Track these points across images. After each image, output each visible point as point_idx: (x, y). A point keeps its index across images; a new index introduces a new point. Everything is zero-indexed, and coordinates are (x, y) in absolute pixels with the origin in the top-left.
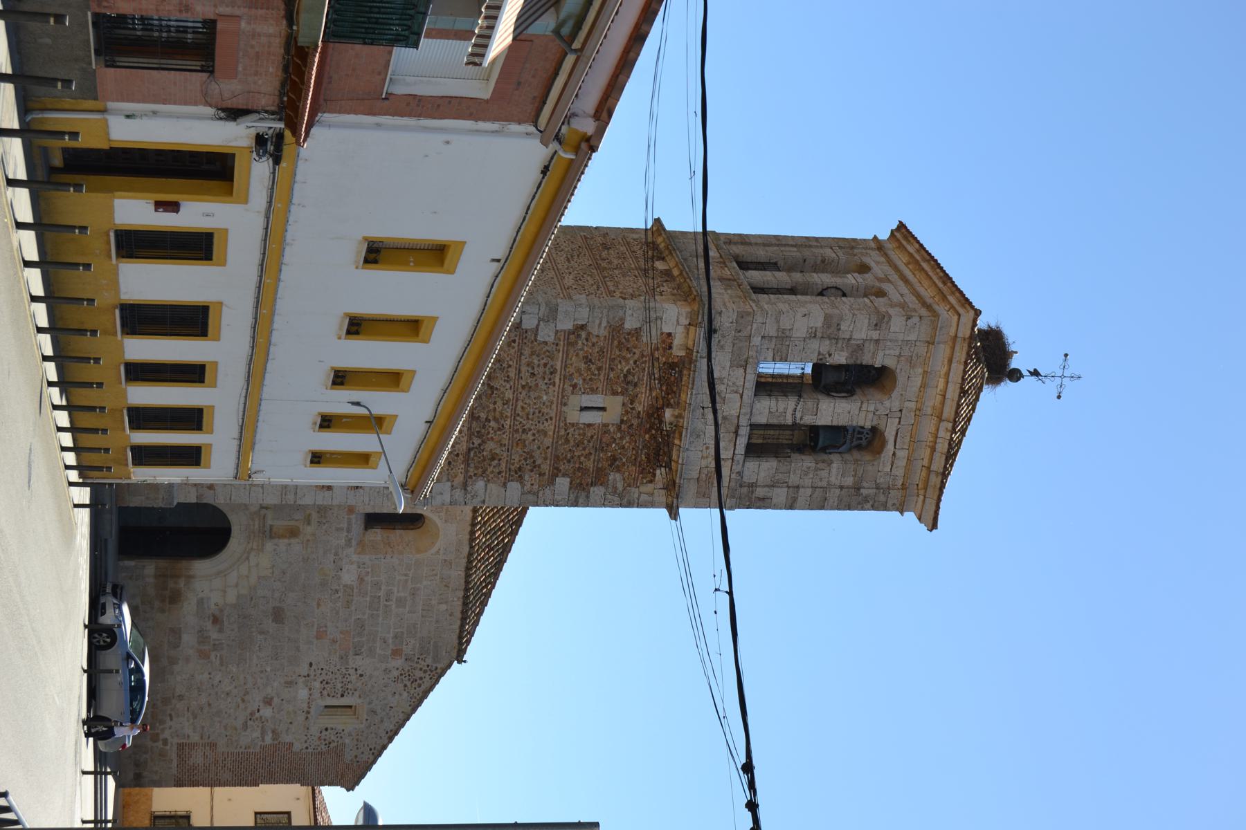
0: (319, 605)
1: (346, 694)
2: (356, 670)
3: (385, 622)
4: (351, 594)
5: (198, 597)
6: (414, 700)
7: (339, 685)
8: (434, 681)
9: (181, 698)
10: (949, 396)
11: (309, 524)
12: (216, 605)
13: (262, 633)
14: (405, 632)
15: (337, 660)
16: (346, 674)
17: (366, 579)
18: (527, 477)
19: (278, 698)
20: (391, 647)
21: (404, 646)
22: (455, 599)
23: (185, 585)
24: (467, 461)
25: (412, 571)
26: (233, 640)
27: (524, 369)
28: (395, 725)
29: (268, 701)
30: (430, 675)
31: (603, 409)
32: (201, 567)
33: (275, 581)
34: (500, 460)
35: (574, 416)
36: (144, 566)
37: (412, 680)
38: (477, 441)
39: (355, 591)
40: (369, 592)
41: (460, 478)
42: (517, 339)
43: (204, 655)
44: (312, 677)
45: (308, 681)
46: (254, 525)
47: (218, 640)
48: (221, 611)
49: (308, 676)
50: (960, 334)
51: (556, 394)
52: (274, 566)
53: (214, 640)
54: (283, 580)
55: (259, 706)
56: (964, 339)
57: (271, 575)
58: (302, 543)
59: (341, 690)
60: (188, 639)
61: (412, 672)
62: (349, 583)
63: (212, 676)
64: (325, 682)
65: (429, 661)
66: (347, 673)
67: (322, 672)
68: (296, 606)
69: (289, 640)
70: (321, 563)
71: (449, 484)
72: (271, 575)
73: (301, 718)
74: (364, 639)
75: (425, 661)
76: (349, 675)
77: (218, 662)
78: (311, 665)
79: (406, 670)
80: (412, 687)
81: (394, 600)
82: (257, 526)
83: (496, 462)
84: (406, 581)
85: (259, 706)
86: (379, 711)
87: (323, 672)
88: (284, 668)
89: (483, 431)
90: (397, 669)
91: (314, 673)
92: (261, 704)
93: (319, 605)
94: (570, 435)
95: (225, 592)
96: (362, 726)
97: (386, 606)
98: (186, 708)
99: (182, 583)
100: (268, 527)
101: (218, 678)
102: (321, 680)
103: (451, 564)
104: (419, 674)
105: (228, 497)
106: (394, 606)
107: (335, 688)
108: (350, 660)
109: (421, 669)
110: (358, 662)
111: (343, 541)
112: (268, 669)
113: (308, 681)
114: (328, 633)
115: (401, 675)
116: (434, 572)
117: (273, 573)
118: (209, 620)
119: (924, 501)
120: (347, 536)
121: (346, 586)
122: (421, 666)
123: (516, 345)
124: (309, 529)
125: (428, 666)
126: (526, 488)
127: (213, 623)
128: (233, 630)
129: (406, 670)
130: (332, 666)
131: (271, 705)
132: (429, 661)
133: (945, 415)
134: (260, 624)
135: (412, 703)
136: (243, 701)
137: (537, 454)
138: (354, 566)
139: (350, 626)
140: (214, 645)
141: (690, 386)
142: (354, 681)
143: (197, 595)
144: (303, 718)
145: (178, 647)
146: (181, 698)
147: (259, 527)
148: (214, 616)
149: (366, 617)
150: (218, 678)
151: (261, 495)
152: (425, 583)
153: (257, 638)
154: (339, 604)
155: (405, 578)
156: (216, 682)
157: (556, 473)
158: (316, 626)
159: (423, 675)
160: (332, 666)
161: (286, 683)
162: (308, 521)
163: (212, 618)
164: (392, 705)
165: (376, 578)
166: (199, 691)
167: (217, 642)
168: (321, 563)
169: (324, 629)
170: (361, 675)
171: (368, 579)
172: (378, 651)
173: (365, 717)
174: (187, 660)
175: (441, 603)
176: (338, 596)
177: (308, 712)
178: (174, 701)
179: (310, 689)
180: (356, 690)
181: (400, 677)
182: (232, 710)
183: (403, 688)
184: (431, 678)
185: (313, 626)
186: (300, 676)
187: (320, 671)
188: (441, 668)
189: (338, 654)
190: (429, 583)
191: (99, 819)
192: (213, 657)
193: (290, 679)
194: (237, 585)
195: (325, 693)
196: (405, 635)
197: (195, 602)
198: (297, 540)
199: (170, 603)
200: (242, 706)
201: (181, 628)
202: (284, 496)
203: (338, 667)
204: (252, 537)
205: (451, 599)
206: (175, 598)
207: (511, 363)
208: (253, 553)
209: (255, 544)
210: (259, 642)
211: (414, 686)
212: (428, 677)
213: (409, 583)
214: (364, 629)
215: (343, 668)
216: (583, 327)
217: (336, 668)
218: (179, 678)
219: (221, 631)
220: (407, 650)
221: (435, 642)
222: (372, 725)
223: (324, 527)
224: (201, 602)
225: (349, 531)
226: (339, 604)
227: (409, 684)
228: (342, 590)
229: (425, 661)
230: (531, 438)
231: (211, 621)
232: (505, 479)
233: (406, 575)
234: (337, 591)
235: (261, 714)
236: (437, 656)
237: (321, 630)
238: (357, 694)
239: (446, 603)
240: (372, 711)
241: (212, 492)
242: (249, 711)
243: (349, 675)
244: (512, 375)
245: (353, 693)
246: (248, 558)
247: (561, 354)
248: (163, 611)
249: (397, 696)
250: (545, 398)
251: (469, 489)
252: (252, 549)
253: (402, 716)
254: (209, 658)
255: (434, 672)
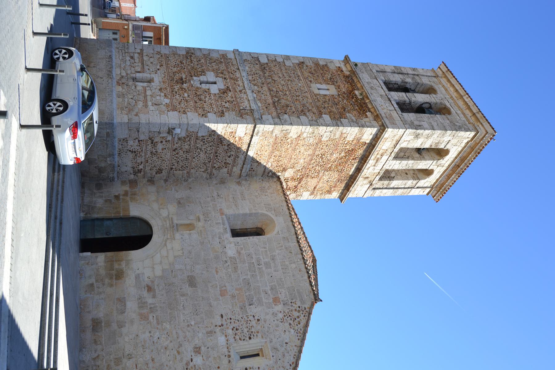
0: (217, 272)
1: (252, 336)
2: (254, 316)
3: (262, 279)
4: (235, 262)
5: (136, 273)
6: (299, 335)
7: (246, 330)
8: (307, 317)
9: (130, 357)
10: (457, 88)
11: (199, 220)
12: (149, 278)
13: (183, 295)
14: (277, 285)
15: (239, 310)
16: (248, 321)
17: (242, 252)
18: (308, 114)
19: (205, 347)
20: (272, 296)
21: (280, 295)
22: (299, 260)
23: (126, 266)
24: (275, 106)
25: (268, 245)
26: (164, 303)
27: (285, 74)
28: (294, 358)
29: (197, 350)
30: (303, 313)
31: (328, 90)
32: (135, 254)
33: (185, 258)
34: (291, 107)
35: (317, 92)
36: (97, 256)
37: (293, 319)
38: (276, 99)
39: (237, 260)
40: (246, 260)
41: (275, 114)
42: (277, 64)
43: (144, 317)
44: (225, 326)
45: (223, 329)
46: (166, 224)
47: (153, 304)
48: (153, 282)
49: (222, 325)
50: (444, 71)
51: (304, 83)
52: (183, 249)
53: (150, 304)
54: (191, 257)
55: (192, 356)
56: (447, 71)
57: (182, 254)
58: (198, 233)
59: (248, 333)
60: (132, 305)
61: (291, 314)
62: (232, 256)
63: (152, 335)
64: (235, 329)
65: (299, 304)
66: (248, 319)
67: (231, 321)
68: (202, 274)
69: (203, 298)
70: (212, 244)
71: (270, 116)
72: (182, 254)
73: (225, 361)
74: (252, 293)
75: (296, 304)
76: (250, 321)
77: (155, 321)
78: (222, 316)
79: (286, 312)
80: (294, 324)
81: (263, 264)
82: (168, 224)
83: (289, 108)
84: (266, 251)
85: (192, 356)
86: (279, 347)
87: (232, 321)
88: (204, 321)
89: (277, 95)
90: (281, 312)
91: (226, 323)
92: (193, 354)
93: (217, 272)
94: (319, 99)
95: (153, 268)
96: (271, 362)
97: (259, 269)
98: (134, 366)
99: (123, 264)
100: (175, 224)
101: (157, 334)
102: (232, 327)
103: (288, 239)
104: (296, 314)
105: (148, 120)
106: (264, 268)
107: (243, 333)
108: (247, 309)
109: (296, 310)
110: (253, 310)
111: (222, 230)
112: (193, 323)
113: (223, 329)
114: (228, 291)
115: (285, 316)
116: (281, 245)
117: (183, 253)
118: (145, 290)
119: (482, 125)
120: (223, 227)
121: (230, 258)
122: (295, 308)
123: (277, 66)
124: (200, 224)
125: (299, 307)
126: (310, 118)
127: (148, 291)
128: (163, 295)
129: (286, 312)
130: (237, 316)
131: (200, 353)
132: (299, 304)
133: (462, 94)
134: (181, 289)
135: (299, 337)
136: (178, 353)
137: (307, 105)
138: (233, 245)
139: (241, 285)
140: (151, 308)
141: (359, 79)
142: (255, 325)
143: (135, 272)
144: (227, 362)
145: (124, 312)
146: (130, 357)
147: (170, 224)
148: (148, 286)
149: (249, 277)
150: (157, 334)
151: (167, 119)
152: (277, 251)
153: (180, 300)
154: (230, 270)
155: (265, 249)
156: (155, 339)
157: (321, 114)
158: (218, 287)
159: (298, 314)
160: (237, 316)
161: (207, 333)
162: (199, 220)
163: (146, 288)
164: (286, 341)
165: (248, 251)
166: (144, 348)
167: (152, 306)
168: (212, 244)
169: (224, 288)
170: (258, 320)
171: (243, 252)
172: (264, 300)
173: (271, 354)
174: (132, 322)
175: (292, 263)
176: (227, 264)
177: (229, 356)
178: (124, 360)
179: (226, 336)
180: (258, 332)
181: (284, 318)
182: (171, 362)
183: (289, 327)
184: (304, 316)
185: (217, 287)
186: (216, 326)
187: (229, 321)
188: (308, 308)
189: (238, 305)
190: (280, 251)
191: (52, 367)
192: (151, 318)
193: (209, 329)
194: (161, 263)
195: (237, 337)
196: (277, 287)
197: (134, 277)
198: (194, 231)
199: (116, 279)
200: (178, 357)
201: (125, 297)
202: (181, 119)
203: (241, 316)
204: (166, 232)
205: (296, 260)
206: (119, 275)
207: (278, 72)
208: (168, 241)
209: (169, 235)
210: (182, 303)
211: (296, 324)
212: (302, 316)
213: (268, 252)
214: (250, 286)
215: (245, 316)
216: (303, 63)
217: (240, 317)
218: (127, 339)
219: (154, 297)
220: (282, 297)
221: (297, 290)
222: (278, 360)
223: (209, 223)
224: (137, 277)
225: (224, 224)
226: (230, 270)
227: (291, 322)
228: (229, 260)
229: (296, 304)
230: (302, 99)
231: (146, 290)
232: (297, 114)
233: (265, 248)
234: (226, 262)
235: (195, 363)
236: (302, 300)
237: (223, 289)
238: (260, 335)
239: (294, 263)
240: (275, 349)
241: (137, 117)
242: (184, 362)
243: (250, 321)
244: (281, 76)
245: (257, 335)
246: (165, 245)
247: (298, 70)
248: (111, 285)
249: (287, 333)
250: (300, 84)
251: (281, 118)
252: (167, 238)
253: (296, 349)
254: (148, 319)
255: (305, 311)
